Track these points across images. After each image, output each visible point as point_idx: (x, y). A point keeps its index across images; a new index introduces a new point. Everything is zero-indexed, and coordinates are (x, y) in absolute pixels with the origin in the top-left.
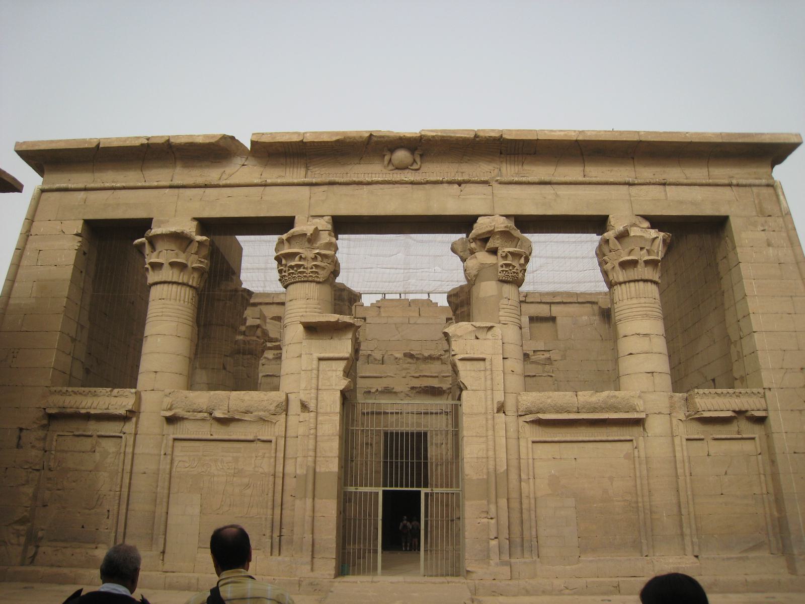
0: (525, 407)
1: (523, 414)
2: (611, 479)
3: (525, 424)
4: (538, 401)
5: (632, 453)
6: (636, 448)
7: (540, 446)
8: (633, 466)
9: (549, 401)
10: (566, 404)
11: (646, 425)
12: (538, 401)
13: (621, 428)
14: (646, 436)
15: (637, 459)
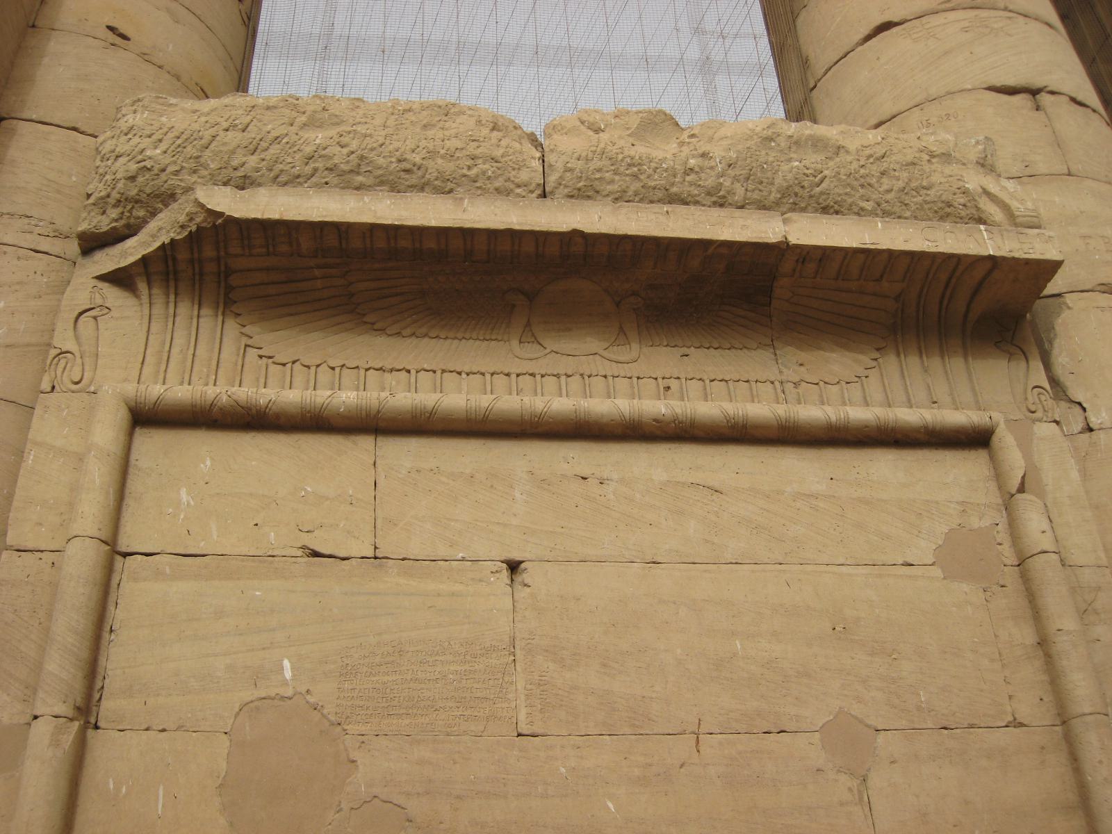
0: (124, 167)
1: (103, 223)
2: (850, 742)
3: (113, 295)
4: (234, 138)
5: (1002, 534)
6: (1021, 489)
7: (206, 451)
8: (1027, 636)
9: (319, 137)
10: (451, 156)
11: (1061, 360)
12: (234, 138)
13: (890, 362)
14: (1078, 426)
15: (1046, 570)
